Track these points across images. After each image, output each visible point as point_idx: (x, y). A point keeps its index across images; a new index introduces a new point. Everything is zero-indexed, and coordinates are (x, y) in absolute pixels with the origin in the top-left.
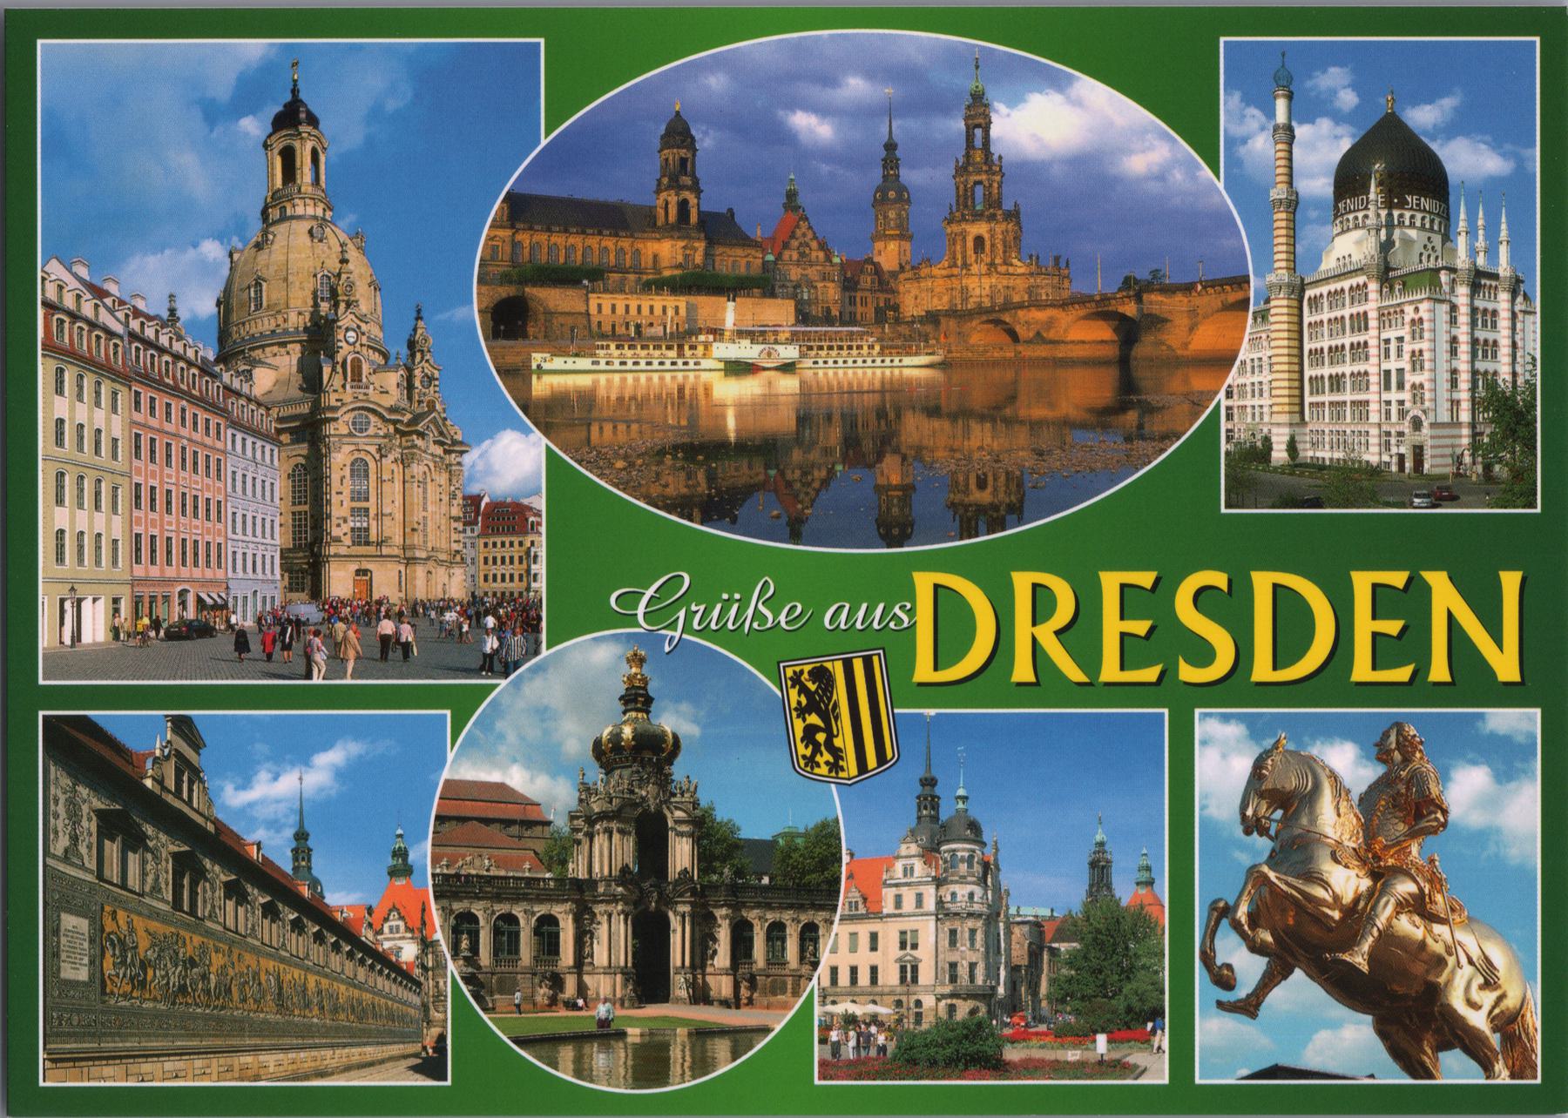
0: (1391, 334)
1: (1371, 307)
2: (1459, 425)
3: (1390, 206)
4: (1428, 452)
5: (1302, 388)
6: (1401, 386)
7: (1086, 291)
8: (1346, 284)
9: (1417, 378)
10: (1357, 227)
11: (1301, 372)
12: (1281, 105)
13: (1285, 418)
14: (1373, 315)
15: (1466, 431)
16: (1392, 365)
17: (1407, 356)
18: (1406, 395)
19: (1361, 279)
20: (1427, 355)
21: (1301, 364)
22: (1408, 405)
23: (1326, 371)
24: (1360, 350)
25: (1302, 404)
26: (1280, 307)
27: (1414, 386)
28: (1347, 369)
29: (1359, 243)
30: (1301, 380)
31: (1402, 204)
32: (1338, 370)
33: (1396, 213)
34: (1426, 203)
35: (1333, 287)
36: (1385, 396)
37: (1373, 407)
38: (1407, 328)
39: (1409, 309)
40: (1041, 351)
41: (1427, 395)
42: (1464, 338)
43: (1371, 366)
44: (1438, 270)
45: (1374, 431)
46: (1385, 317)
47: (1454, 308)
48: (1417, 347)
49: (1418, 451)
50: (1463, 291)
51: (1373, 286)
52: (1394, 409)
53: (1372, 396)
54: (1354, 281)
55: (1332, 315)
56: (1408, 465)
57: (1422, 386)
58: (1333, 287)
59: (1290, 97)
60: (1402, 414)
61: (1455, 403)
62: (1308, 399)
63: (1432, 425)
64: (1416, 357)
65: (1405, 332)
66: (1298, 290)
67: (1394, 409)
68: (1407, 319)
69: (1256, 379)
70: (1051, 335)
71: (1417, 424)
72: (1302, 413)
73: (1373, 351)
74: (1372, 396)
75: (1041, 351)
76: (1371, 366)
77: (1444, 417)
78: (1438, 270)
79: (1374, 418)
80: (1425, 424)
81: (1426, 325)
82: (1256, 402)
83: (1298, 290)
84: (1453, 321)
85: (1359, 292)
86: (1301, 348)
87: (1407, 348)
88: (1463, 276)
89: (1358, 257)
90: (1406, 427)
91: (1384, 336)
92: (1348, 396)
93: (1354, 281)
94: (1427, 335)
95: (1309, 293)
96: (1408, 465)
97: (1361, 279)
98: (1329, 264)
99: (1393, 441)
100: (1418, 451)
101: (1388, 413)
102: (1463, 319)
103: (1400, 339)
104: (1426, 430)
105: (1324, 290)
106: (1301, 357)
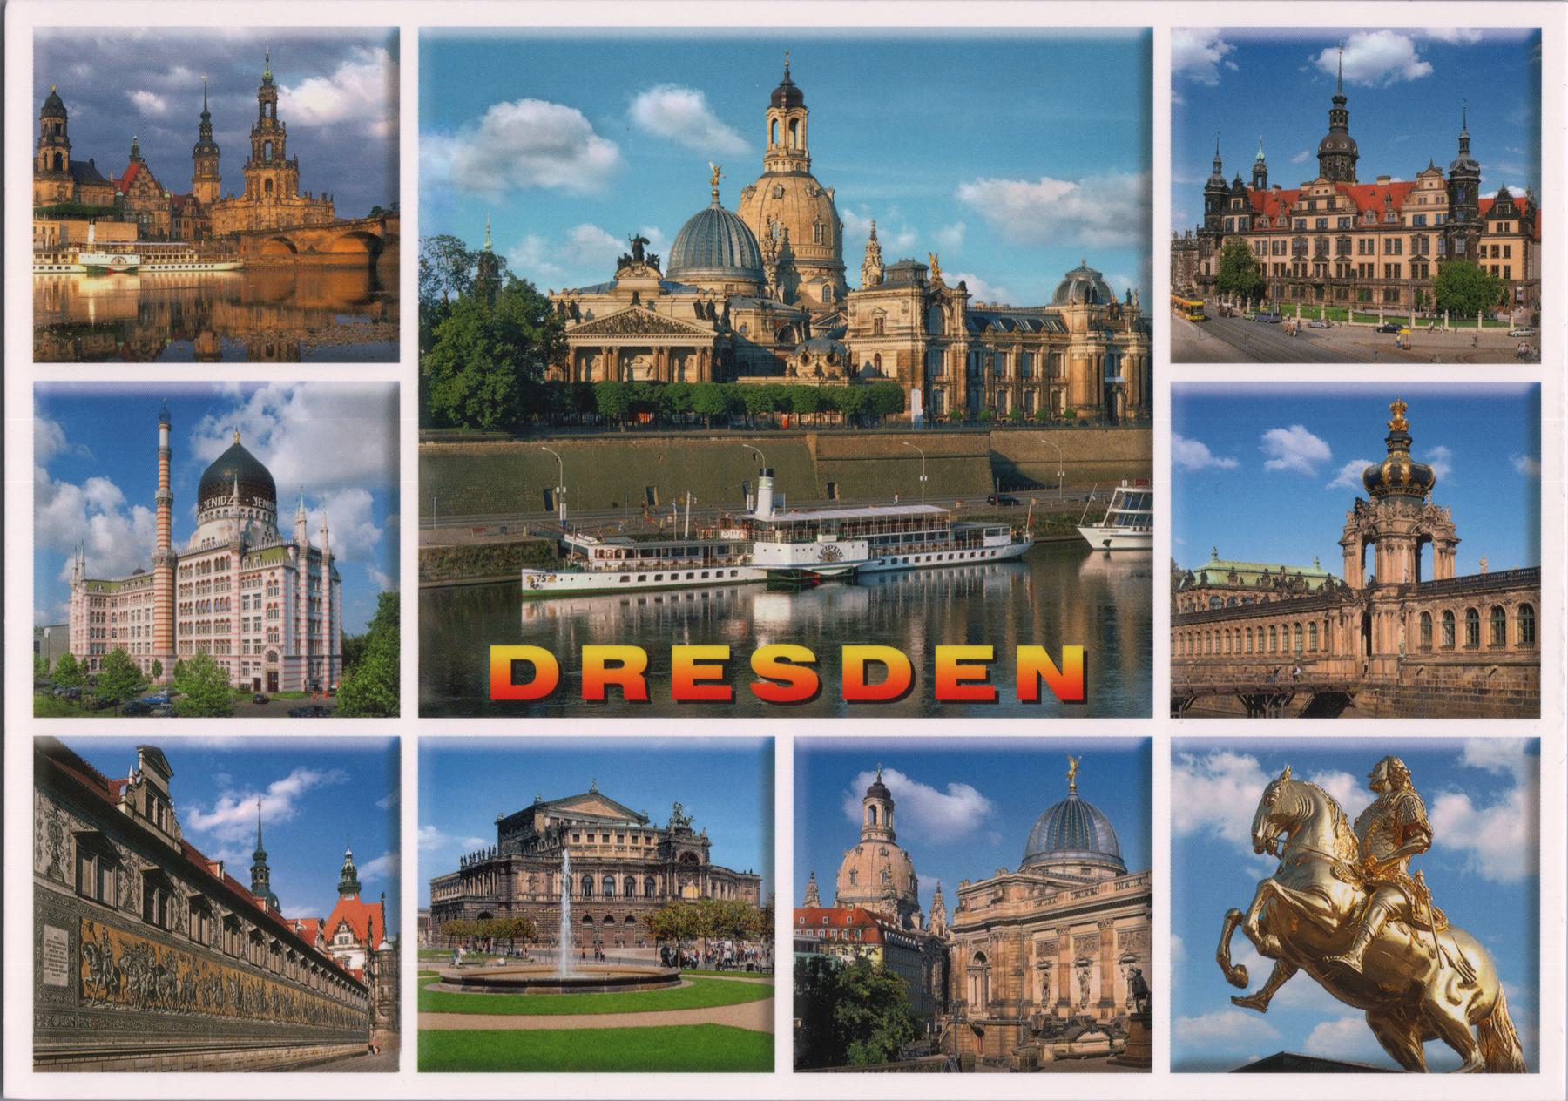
0: (250, 592)
1: (233, 572)
2: (300, 658)
3: (242, 502)
4: (281, 677)
5: (174, 631)
6: (257, 628)
7: (345, 217)
8: (212, 557)
9: (272, 624)
10: (219, 518)
11: (174, 619)
12: (163, 434)
13: (164, 652)
14: (234, 578)
15: (304, 662)
16: (251, 613)
17: (264, 608)
18: (262, 636)
19: (225, 554)
20: (281, 607)
21: (174, 614)
22: (264, 643)
23: (194, 618)
24: (223, 604)
25: (174, 642)
26: (160, 573)
27: (269, 629)
28: (212, 617)
29: (222, 529)
30: (174, 625)
31: (251, 504)
32: (205, 618)
33: (247, 509)
34: (266, 504)
35: (200, 559)
36: (244, 637)
37: (234, 644)
38: (264, 587)
39: (266, 576)
40: (312, 260)
41: (281, 636)
42: (303, 596)
43: (233, 615)
44: (287, 547)
45: (234, 662)
46: (243, 580)
47: (298, 575)
48: (272, 601)
49: (272, 676)
50: (303, 562)
51: (235, 558)
52: (252, 645)
53: (233, 636)
54: (219, 555)
55: (219, 575)
56: (264, 686)
57: (276, 629)
58: (200, 559)
59: (169, 429)
60: (257, 649)
61: (298, 642)
62: (178, 639)
63: (286, 658)
64: (272, 610)
65: (262, 590)
66: (172, 562)
67: (252, 645)
68: (265, 581)
69: (136, 624)
70: (320, 248)
71: (272, 657)
72: (174, 647)
73: (234, 604)
74: (233, 636)
75: (312, 260)
76: (233, 615)
77: (293, 653)
78: (287, 547)
79: (234, 652)
80: (280, 657)
81: (281, 585)
82: (136, 641)
83: (172, 562)
84: (297, 584)
85: (222, 564)
86: (174, 602)
87: (264, 601)
88: (303, 554)
89: (221, 538)
90: (263, 660)
91: (244, 593)
92: (213, 637)
93: (219, 555)
94: (281, 592)
95: (182, 564)
96: (264, 686)
97: (225, 554)
98: (195, 543)
99: (251, 668)
100: (272, 676)
101: (246, 649)
102: (303, 582)
103: (258, 595)
104: (281, 661)
105: (194, 561)
106: (174, 608)
